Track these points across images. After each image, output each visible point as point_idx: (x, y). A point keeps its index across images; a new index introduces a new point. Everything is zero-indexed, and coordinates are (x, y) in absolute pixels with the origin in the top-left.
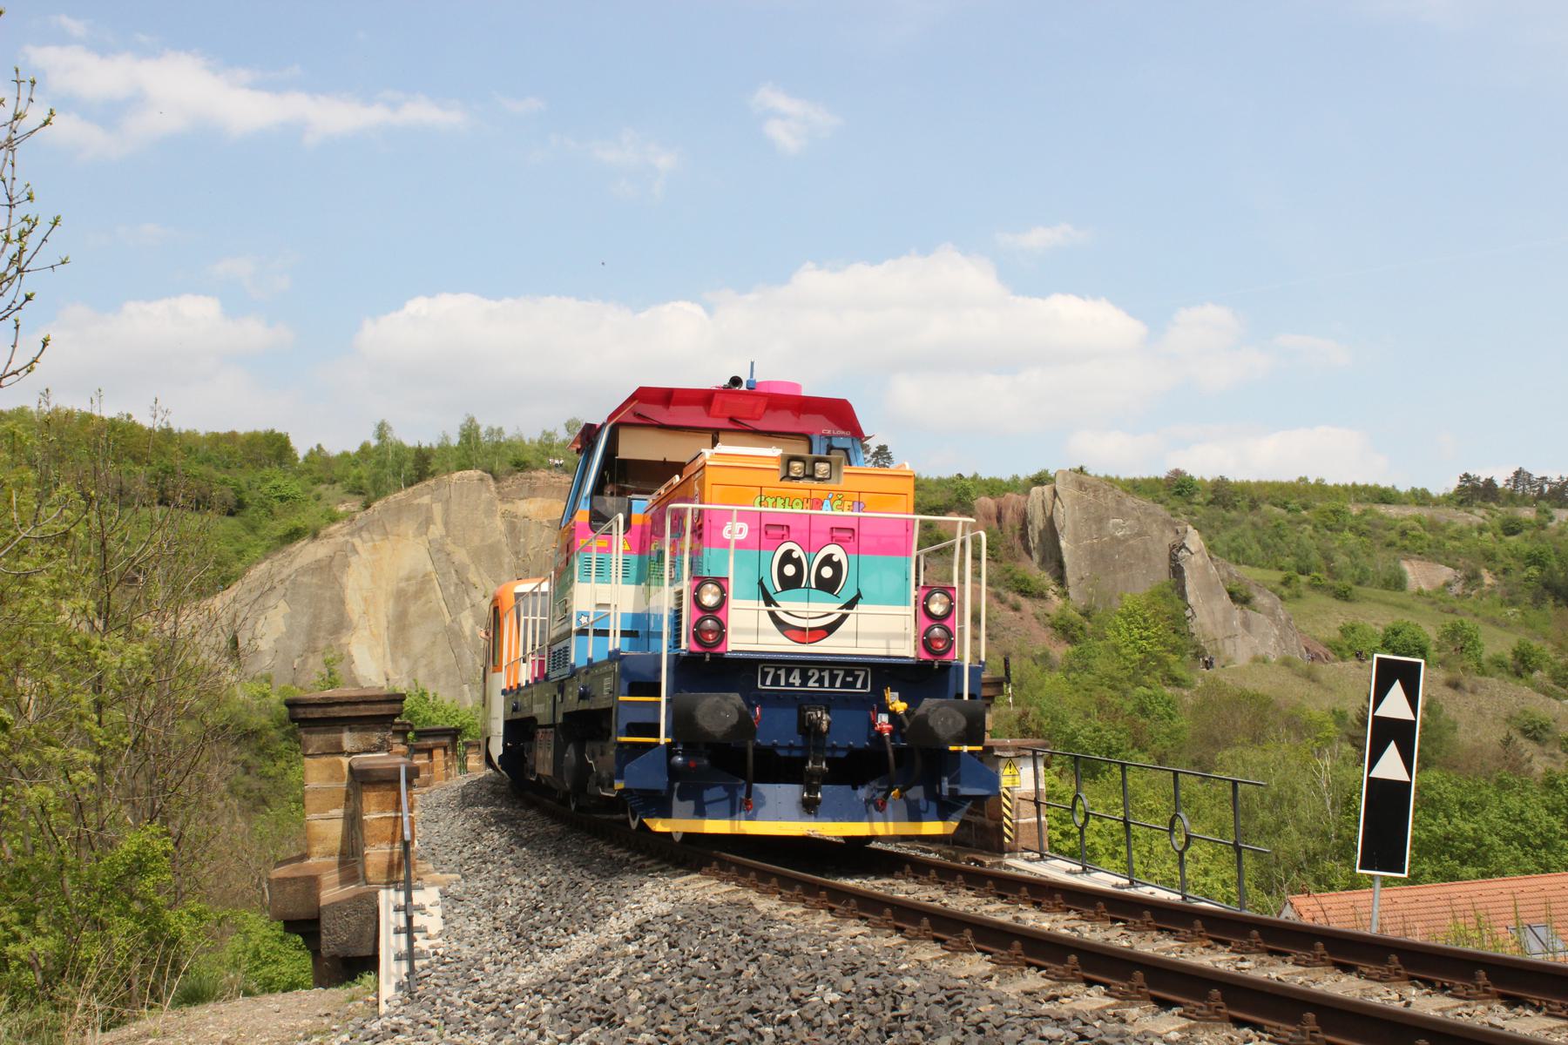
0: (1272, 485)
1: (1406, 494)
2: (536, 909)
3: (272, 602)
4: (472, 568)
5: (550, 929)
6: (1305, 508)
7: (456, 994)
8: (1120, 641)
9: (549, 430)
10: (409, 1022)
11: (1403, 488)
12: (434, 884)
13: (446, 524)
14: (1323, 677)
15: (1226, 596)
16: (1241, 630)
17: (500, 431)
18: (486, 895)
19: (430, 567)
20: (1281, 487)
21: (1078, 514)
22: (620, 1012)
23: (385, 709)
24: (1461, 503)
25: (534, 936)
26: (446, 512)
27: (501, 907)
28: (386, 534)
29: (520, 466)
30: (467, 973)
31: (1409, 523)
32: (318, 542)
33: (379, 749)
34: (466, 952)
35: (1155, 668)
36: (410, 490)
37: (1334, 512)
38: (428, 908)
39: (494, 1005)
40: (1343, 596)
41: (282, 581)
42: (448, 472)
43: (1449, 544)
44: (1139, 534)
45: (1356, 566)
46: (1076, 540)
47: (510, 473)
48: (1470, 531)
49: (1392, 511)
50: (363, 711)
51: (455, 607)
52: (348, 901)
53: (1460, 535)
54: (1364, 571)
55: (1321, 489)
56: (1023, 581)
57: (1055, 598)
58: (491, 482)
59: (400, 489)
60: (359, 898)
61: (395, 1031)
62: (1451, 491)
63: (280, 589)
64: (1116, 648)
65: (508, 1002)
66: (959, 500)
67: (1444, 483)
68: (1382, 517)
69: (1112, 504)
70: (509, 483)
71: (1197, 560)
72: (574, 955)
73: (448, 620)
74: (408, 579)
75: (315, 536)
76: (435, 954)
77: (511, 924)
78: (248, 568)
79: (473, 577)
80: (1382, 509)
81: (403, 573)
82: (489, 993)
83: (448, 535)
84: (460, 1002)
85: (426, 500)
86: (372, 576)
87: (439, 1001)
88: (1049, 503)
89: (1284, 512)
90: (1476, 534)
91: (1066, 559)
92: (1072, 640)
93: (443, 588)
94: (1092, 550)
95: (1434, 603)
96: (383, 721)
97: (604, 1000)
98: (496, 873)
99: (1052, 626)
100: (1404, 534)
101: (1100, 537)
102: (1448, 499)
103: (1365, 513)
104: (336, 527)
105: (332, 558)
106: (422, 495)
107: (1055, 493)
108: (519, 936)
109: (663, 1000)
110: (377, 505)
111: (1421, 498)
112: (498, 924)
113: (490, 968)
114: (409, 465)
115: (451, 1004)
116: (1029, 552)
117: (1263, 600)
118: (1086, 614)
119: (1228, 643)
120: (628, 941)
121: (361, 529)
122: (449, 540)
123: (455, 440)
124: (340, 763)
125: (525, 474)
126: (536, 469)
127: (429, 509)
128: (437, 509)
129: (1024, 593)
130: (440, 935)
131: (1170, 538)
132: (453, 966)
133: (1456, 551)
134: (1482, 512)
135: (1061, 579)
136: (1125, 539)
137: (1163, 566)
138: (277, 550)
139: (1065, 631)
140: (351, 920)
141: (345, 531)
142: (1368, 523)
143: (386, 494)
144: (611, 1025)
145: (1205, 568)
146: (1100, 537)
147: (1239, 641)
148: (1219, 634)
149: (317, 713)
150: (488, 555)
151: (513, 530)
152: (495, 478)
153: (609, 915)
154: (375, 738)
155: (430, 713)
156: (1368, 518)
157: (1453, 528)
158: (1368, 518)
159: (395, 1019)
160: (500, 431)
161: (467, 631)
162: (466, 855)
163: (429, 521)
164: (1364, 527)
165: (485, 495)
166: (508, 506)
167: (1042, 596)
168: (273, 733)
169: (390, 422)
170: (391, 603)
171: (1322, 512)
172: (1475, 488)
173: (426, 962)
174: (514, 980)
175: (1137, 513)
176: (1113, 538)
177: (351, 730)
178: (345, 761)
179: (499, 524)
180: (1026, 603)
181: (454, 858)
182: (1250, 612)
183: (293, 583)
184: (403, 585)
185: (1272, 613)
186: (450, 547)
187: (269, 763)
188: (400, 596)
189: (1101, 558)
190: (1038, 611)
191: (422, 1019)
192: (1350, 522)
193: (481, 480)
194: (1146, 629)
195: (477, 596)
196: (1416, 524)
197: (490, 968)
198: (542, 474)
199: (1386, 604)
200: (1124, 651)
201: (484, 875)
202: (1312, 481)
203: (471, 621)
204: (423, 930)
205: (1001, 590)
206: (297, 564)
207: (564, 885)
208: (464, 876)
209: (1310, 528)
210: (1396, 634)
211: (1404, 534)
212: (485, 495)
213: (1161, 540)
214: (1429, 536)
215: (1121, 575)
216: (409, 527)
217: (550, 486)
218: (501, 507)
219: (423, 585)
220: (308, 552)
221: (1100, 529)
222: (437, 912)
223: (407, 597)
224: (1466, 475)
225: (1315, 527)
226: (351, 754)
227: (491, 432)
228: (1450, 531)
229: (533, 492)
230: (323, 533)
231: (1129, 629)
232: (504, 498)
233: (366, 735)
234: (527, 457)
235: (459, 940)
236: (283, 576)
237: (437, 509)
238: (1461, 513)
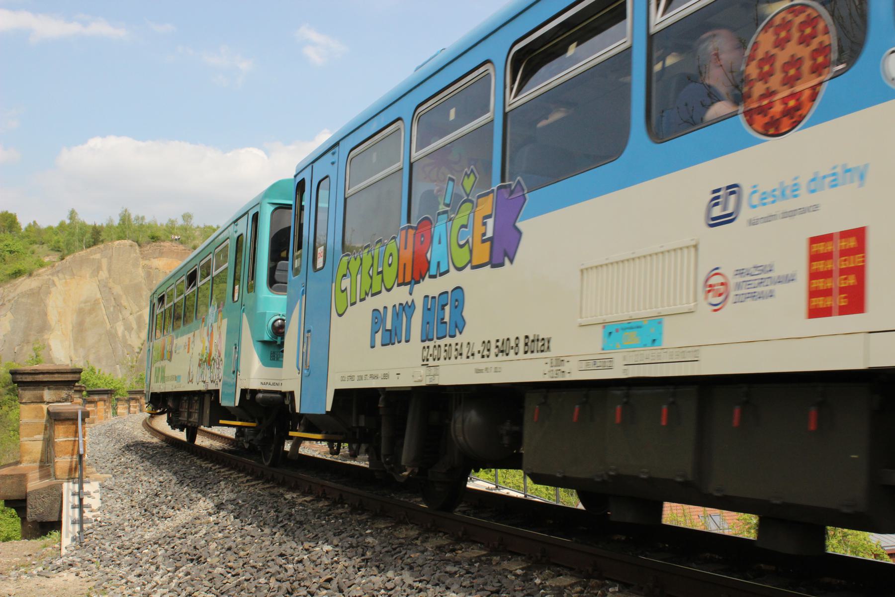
2: (156, 495)
4: (124, 297)
5: (164, 507)
7: (107, 544)
9: (173, 219)
10: (79, 560)
12: (96, 480)
13: (109, 271)
17: (143, 218)
18: (127, 487)
19: (99, 296)
22: (204, 555)
23: (70, 377)
25: (155, 511)
27: (136, 494)
28: (73, 275)
29: (154, 239)
30: (115, 531)
32: (32, 278)
33: (66, 400)
34: (114, 519)
36: (88, 250)
38: (92, 494)
39: (130, 551)
41: (9, 301)
42: (112, 240)
47: (148, 243)
50: (57, 378)
52: (45, 489)
58: (137, 247)
60: (51, 487)
61: (71, 565)
63: (8, 305)
65: (138, 549)
72: (178, 522)
73: (108, 327)
74: (86, 302)
75: (30, 275)
76: (96, 520)
77: (141, 504)
79: (124, 303)
82: (127, 543)
84: (110, 549)
85: (98, 256)
87: (97, 548)
93: (106, 308)
96: (69, 384)
97: (195, 548)
98: (133, 474)
105: (40, 288)
106: (95, 253)
108: (146, 510)
109: (229, 549)
110: (68, 258)
112: (134, 503)
113: (128, 529)
114: (88, 235)
115: (104, 549)
120: (210, 514)
121: (58, 272)
122: (111, 281)
123: (116, 221)
124: (42, 408)
126: (164, 241)
128: (105, 262)
130: (99, 510)
132: (106, 528)
138: (6, 282)
140: (46, 500)
141: (49, 272)
143: (74, 252)
144: (199, 563)
149: (29, 378)
151: (149, 275)
152: (139, 245)
153: (199, 500)
154: (64, 393)
155: (96, 382)
159: (71, 558)
160: (143, 218)
161: (120, 333)
162: (115, 463)
163: (99, 268)
165: (133, 255)
166: (147, 262)
169: (76, 211)
173: (90, 525)
174: (142, 536)
177: (49, 389)
178: (45, 407)
179: (141, 272)
181: (109, 465)
184: (82, 305)
186: (111, 284)
188: (80, 312)
191: (87, 558)
195: (126, 313)
197: (128, 529)
198: (167, 244)
201: (126, 475)
204: (89, 506)
206: (19, 290)
207: (173, 482)
208: (114, 476)
212: (133, 255)
218: (142, 262)
219: (94, 307)
220: (25, 284)
222: (98, 496)
226: (49, 403)
227: (137, 218)
229: (161, 254)
230: (35, 273)
232: (144, 257)
233: (58, 392)
234: (156, 235)
235: (110, 513)
236: (10, 298)
237: (105, 262)
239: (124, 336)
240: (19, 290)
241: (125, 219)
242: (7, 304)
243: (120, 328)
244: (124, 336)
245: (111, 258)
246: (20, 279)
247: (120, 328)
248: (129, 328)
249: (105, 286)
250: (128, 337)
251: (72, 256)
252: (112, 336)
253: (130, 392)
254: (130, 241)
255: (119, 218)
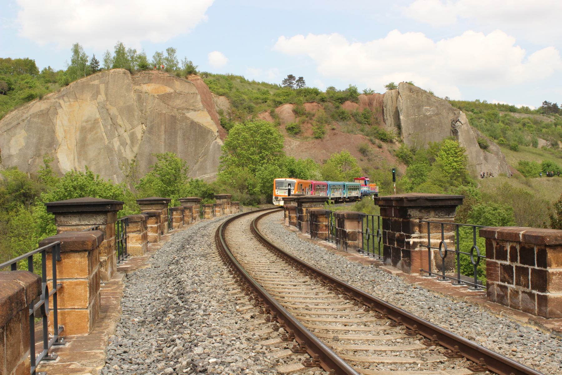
0: (465, 102)
1: (521, 109)
3: (18, 130)
4: (119, 117)
6: (481, 113)
8: (442, 163)
9: (160, 51)
11: (518, 106)
13: (106, 95)
14: (533, 185)
15: (477, 145)
16: (484, 162)
17: (135, 51)
19: (98, 116)
20: (469, 103)
21: (409, 104)
24: (543, 113)
26: (107, 89)
28: (76, 98)
31: (526, 120)
32: (42, 101)
35: (458, 177)
36: (89, 77)
37: (493, 114)
40: (514, 149)
41: (23, 121)
43: (544, 130)
44: (437, 114)
45: (516, 136)
46: (408, 116)
47: (139, 71)
48: (551, 125)
49: (517, 115)
51: (110, 136)
53: (548, 126)
54: (520, 138)
55: (485, 106)
56: (383, 134)
57: (397, 143)
58: (129, 75)
59: (82, 76)
62: (537, 109)
64: (441, 166)
66: (351, 95)
67: (535, 105)
68: (513, 117)
69: (425, 99)
70: (138, 76)
71: (464, 127)
73: (107, 142)
74: (87, 121)
75: (41, 98)
78: (6, 114)
79: (119, 121)
80: (512, 114)
81: (85, 118)
83: (107, 100)
85: (96, 82)
86: (69, 119)
88: (394, 98)
89: (472, 114)
90: (554, 126)
91: (403, 125)
92: (407, 163)
93: (105, 126)
94: (415, 121)
95: (553, 154)
99: (397, 156)
100: (524, 125)
101: (419, 115)
102: (537, 112)
103: (506, 116)
104: (52, 94)
105: (49, 110)
106: (94, 80)
107: (399, 93)
110: (71, 84)
111: (526, 110)
116: (384, 121)
117: (493, 147)
118: (413, 151)
119: (478, 167)
121: (63, 96)
122: (108, 103)
123: (113, 55)
125: (147, 72)
126: (152, 69)
127: (98, 87)
128: (102, 87)
129: (383, 140)
131: (451, 117)
133: (547, 133)
134: (553, 118)
135: (400, 134)
136: (431, 117)
137: (448, 129)
138: (22, 105)
139: (405, 159)
141: (56, 96)
142: (508, 120)
143: (76, 79)
145: (468, 131)
146: (419, 115)
147: (483, 166)
148: (475, 162)
150: (128, 111)
151: (140, 99)
152: (131, 73)
155: (93, 188)
156: (508, 117)
157: (544, 123)
158: (508, 117)
160: (135, 51)
161: (116, 148)
163: (98, 93)
164: (507, 121)
166: (137, 87)
167: (391, 142)
168: (8, 196)
169: (80, 44)
170: (78, 134)
171: (489, 114)
172: (549, 108)
175: (436, 104)
176: (425, 116)
179: (133, 96)
180: (384, 145)
182: (487, 153)
183: (29, 121)
184: (85, 124)
185: (497, 154)
186: (109, 106)
187: (5, 213)
188: (83, 130)
189: (419, 125)
190: (390, 149)
192: (501, 119)
193: (125, 73)
194: (457, 157)
195: (121, 131)
196: (529, 121)
198: (155, 72)
199: (533, 153)
200: (445, 168)
202: (481, 101)
203: (118, 143)
205: (372, 138)
206: (32, 111)
209: (484, 121)
210: (548, 166)
211: (524, 125)
212: (127, 81)
213: (447, 118)
214: (535, 126)
215: (428, 133)
216: (88, 96)
217: (158, 78)
220: (36, 106)
221: (419, 111)
223: (86, 131)
224: (546, 102)
225: (486, 120)
227: (130, 51)
228: (543, 125)
229: (150, 80)
230: (45, 97)
231: (447, 158)
232: (136, 83)
236: (24, 118)
237: (102, 87)
238: (545, 118)
239: (119, 150)
240: (32, 111)
241: (120, 52)
242: (22, 123)
243: (116, 144)
244: (119, 150)
245: (107, 83)
246: (32, 102)
247: (116, 144)
248: (123, 144)
249: (103, 108)
250: (123, 151)
251: (75, 82)
252: (109, 150)
253: (142, 203)
254: (124, 70)
255: (114, 50)
